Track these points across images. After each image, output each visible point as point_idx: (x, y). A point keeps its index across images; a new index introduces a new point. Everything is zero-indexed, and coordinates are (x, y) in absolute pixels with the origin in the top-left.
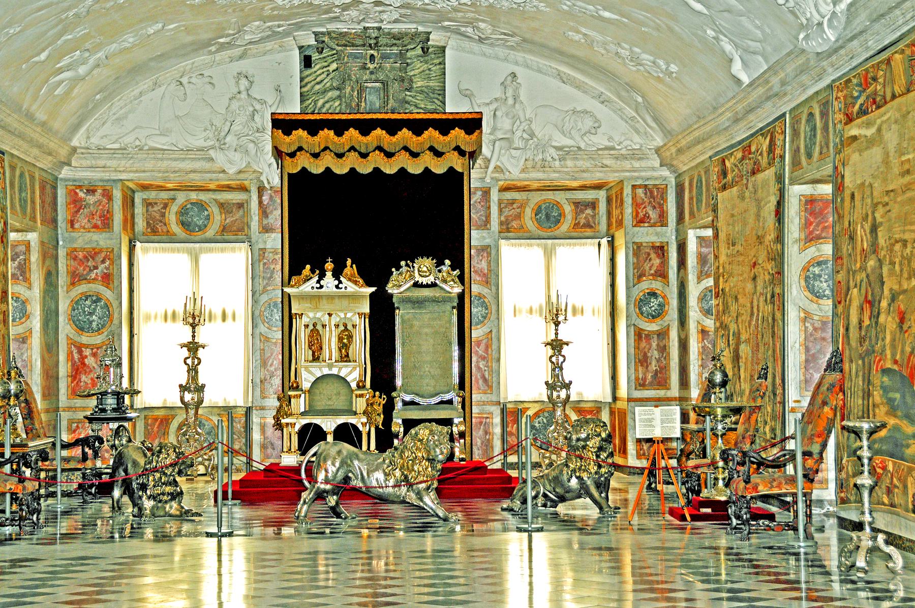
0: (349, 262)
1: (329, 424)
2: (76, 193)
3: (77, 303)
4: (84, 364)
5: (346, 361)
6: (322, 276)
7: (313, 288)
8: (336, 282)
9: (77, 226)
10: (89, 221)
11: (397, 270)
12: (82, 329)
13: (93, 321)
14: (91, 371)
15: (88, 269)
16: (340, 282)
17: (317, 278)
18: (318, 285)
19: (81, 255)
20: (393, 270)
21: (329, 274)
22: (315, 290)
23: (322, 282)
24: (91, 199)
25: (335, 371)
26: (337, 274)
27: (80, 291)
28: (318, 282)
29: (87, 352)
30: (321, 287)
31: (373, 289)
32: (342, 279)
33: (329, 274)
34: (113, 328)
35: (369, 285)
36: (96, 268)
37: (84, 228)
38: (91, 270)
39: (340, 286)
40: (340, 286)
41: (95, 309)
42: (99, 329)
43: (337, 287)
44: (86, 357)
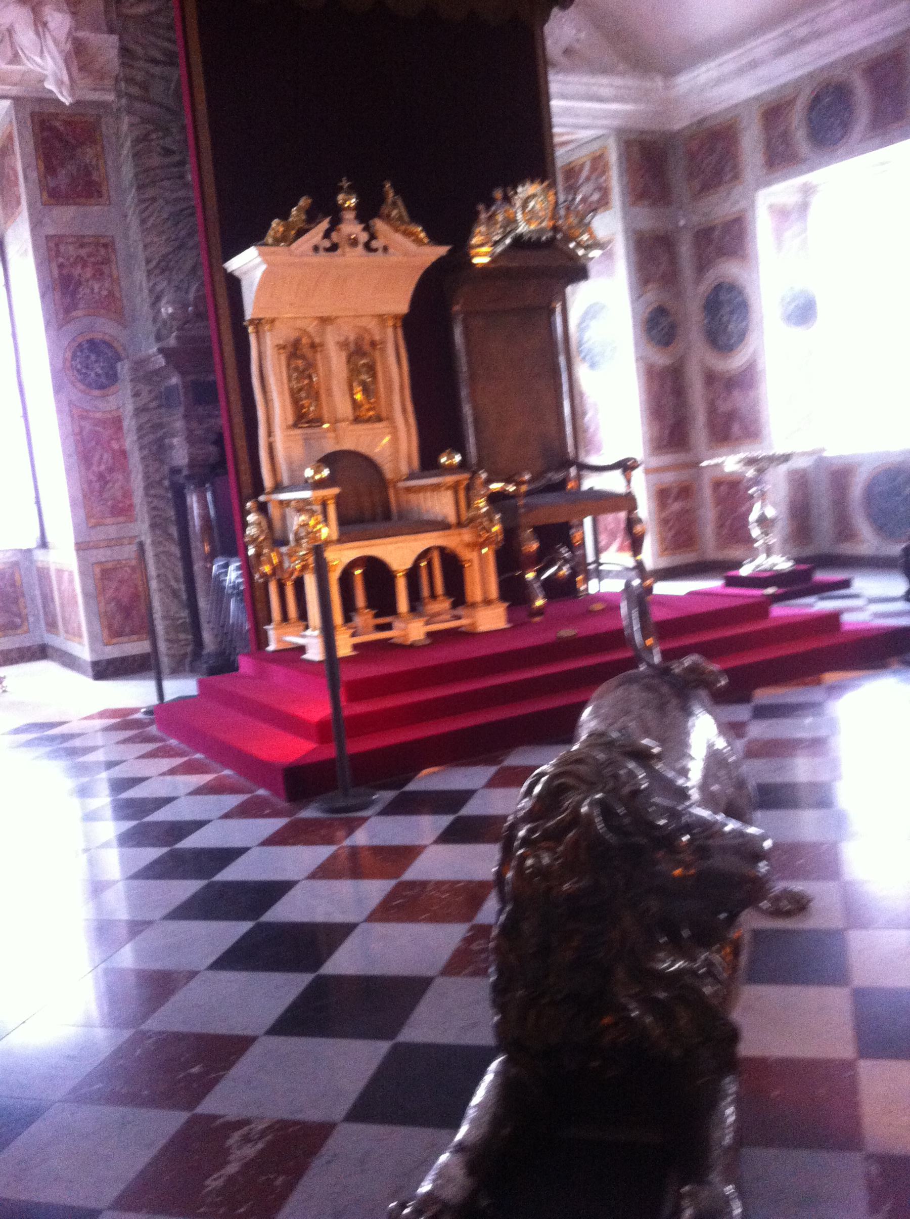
1: (398, 553)
5: (369, 420)
7: (316, 249)
17: (325, 225)
18: (327, 244)
21: (350, 216)
22: (322, 253)
23: (334, 235)
25: (348, 445)
26: (365, 215)
28: (327, 235)
30: (334, 248)
31: (442, 250)
32: (379, 225)
35: (436, 238)
39: (374, 244)
40: (374, 244)
43: (368, 247)
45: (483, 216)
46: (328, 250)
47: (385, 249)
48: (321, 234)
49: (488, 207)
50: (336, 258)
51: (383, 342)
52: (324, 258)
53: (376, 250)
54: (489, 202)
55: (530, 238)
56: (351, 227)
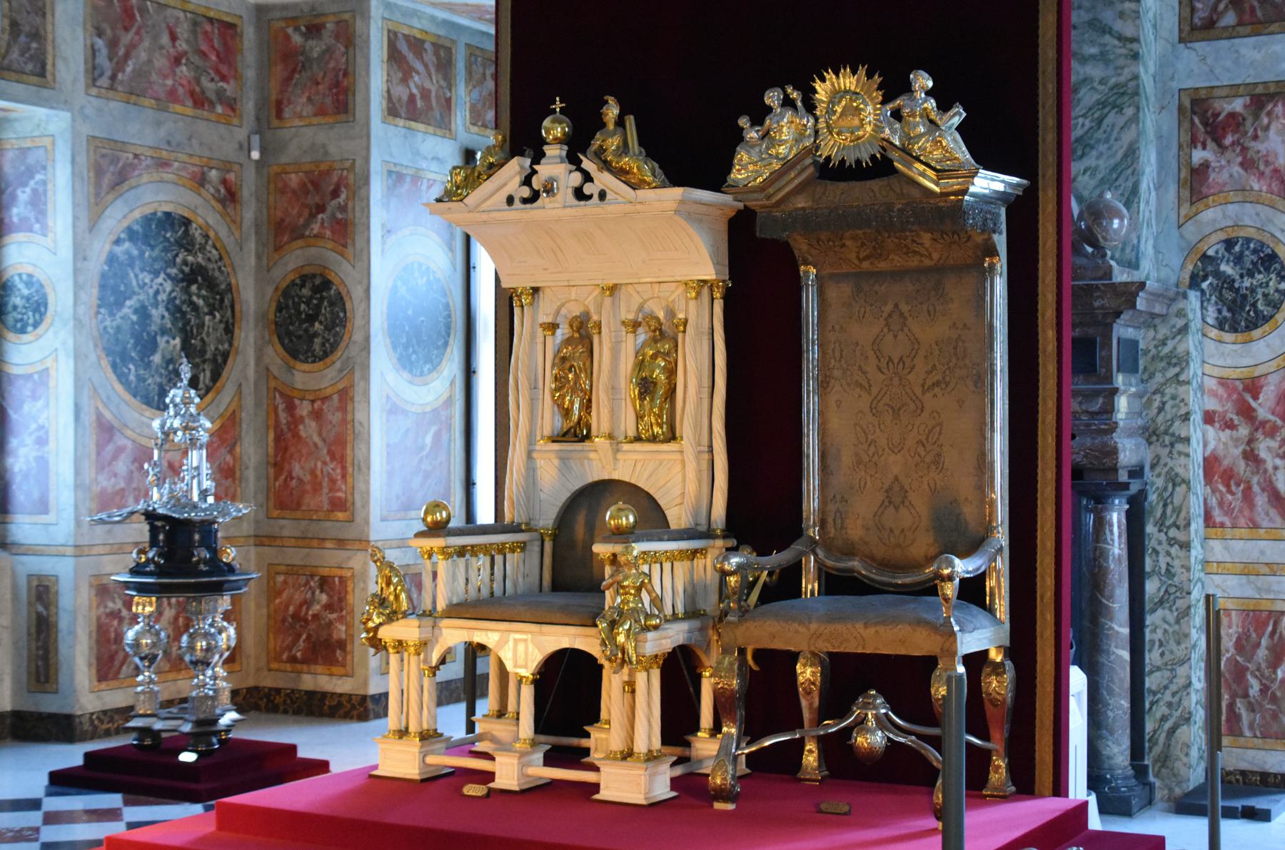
0: (612, 111)
2: (288, 37)
3: (286, 293)
4: (296, 435)
6: (538, 157)
7: (510, 200)
8: (577, 178)
9: (287, 113)
10: (309, 99)
11: (758, 121)
12: (294, 354)
13: (316, 335)
14: (310, 454)
15: (306, 213)
16: (588, 178)
18: (526, 192)
19: (294, 180)
20: (744, 122)
21: (554, 152)
24: (316, 48)
26: (576, 148)
27: (291, 266)
28: (527, 181)
29: (304, 409)
30: (535, 196)
32: (587, 164)
33: (554, 152)
34: (354, 351)
36: (321, 208)
37: (301, 117)
38: (312, 216)
39: (588, 189)
41: (318, 307)
42: (326, 355)
43: (579, 194)
44: (302, 419)
45: (752, 135)
46: (525, 201)
47: (602, 195)
48: (517, 180)
49: (758, 121)
50: (532, 212)
51: (685, 323)
52: (520, 213)
53: (590, 197)
54: (760, 114)
55: (843, 161)
56: (554, 167)
